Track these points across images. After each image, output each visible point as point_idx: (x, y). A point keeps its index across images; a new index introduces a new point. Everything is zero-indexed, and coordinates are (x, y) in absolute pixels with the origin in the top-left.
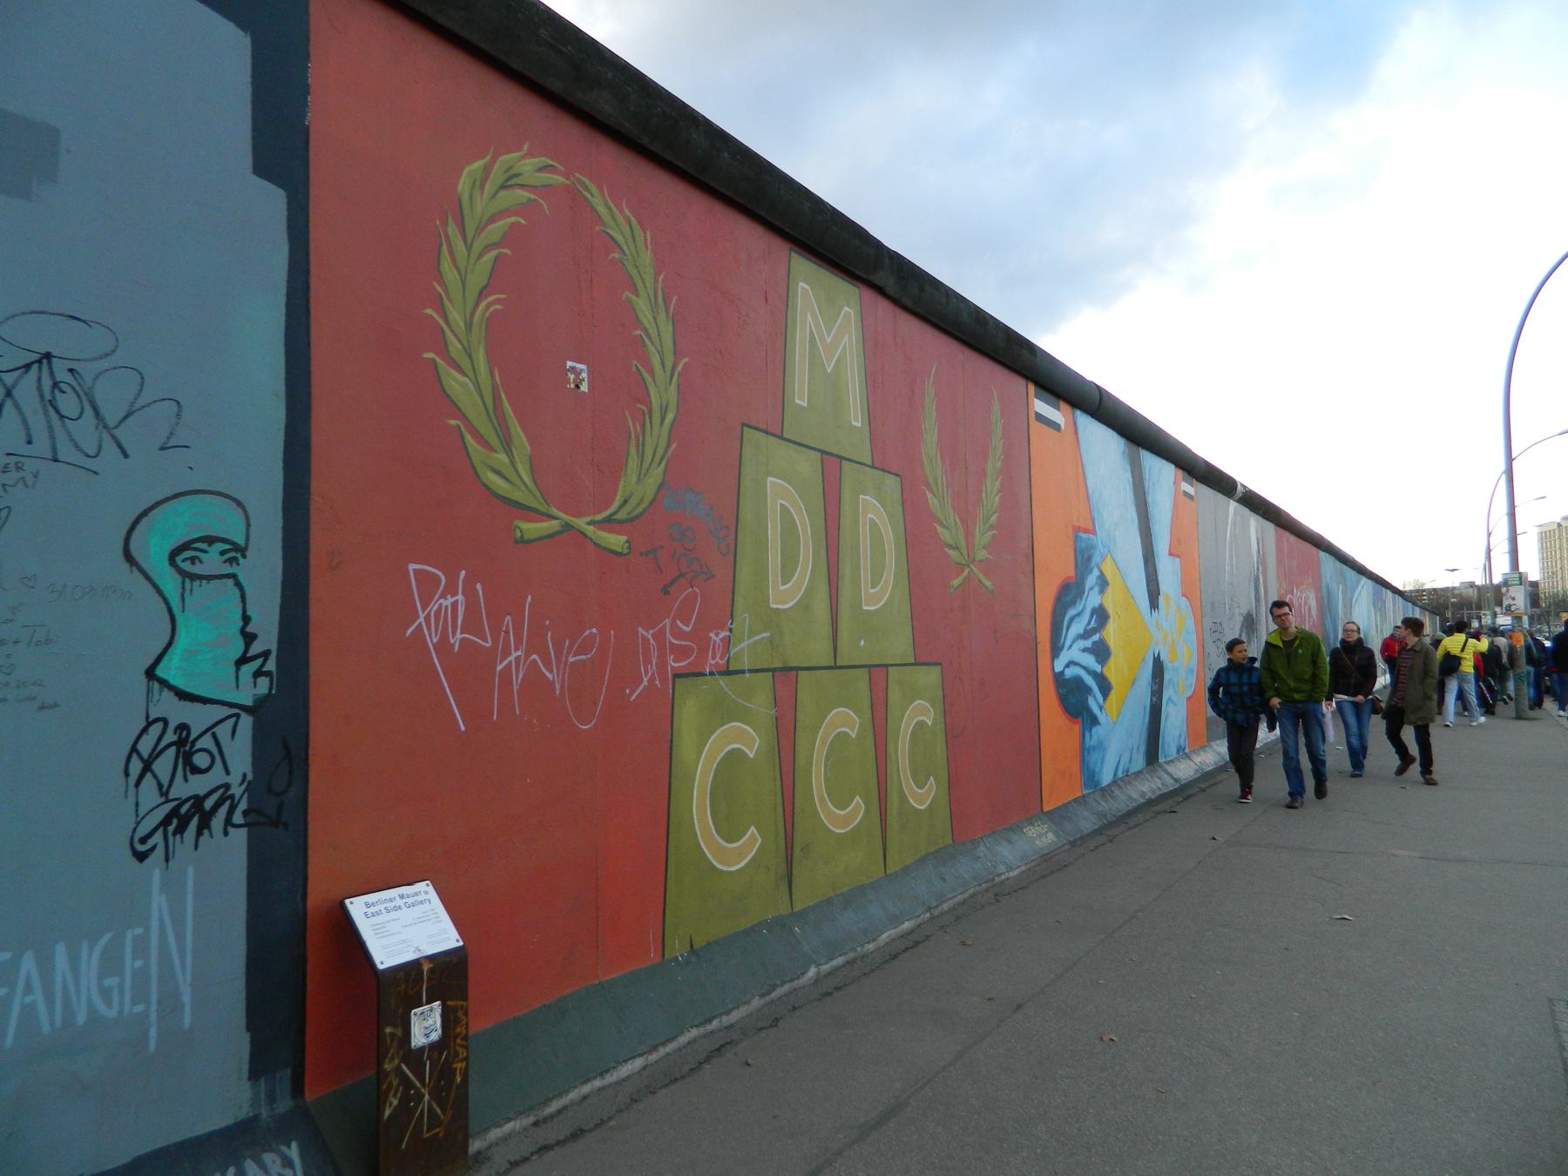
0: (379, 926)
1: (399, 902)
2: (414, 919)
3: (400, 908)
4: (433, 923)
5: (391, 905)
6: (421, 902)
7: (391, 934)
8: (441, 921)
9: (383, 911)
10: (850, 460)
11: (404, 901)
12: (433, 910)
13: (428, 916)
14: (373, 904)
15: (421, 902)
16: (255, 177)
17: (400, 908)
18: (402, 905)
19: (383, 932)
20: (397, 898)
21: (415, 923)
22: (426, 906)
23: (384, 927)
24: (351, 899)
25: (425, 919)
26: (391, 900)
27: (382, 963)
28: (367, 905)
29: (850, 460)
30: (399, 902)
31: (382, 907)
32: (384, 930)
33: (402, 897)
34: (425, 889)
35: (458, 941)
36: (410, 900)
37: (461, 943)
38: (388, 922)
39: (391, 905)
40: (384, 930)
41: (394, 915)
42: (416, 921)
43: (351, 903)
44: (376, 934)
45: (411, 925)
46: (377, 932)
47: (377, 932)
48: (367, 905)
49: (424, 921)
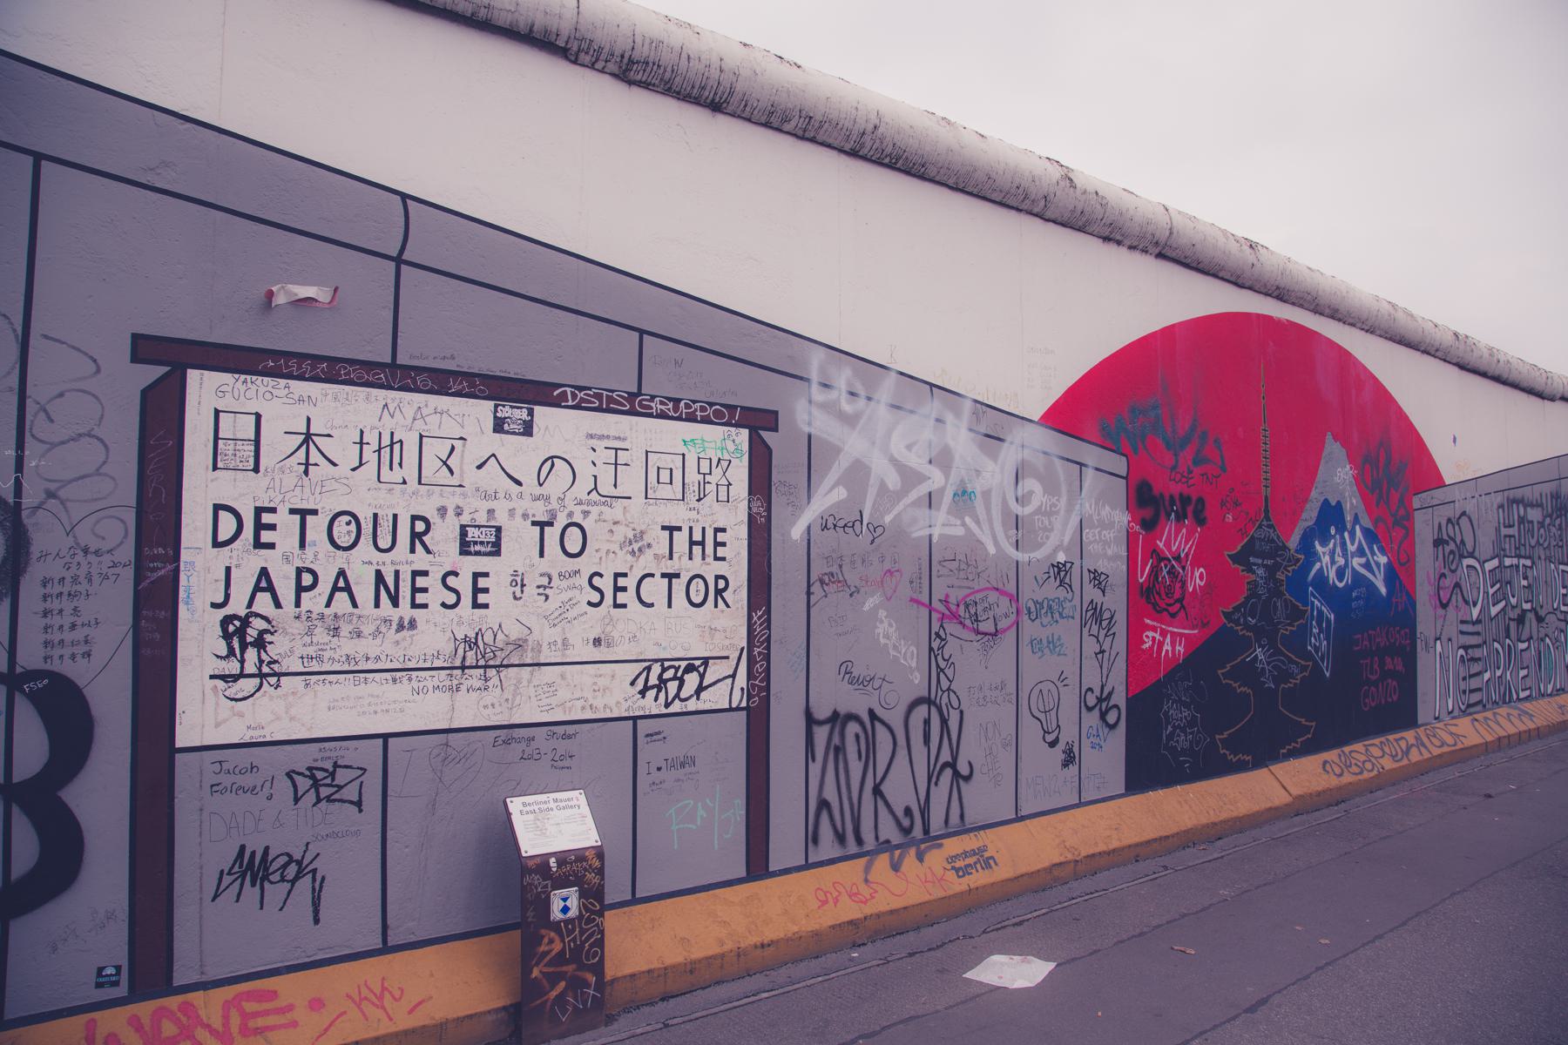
1: (552, 805)
3: (552, 809)
10: (728, 466)
17: (552, 809)
20: (551, 801)
22: (575, 810)
24: (512, 799)
26: (545, 802)
27: (526, 852)
29: (728, 466)
30: (552, 805)
31: (536, 808)
34: (578, 797)
35: (597, 842)
37: (599, 844)
43: (512, 802)
48: (524, 804)
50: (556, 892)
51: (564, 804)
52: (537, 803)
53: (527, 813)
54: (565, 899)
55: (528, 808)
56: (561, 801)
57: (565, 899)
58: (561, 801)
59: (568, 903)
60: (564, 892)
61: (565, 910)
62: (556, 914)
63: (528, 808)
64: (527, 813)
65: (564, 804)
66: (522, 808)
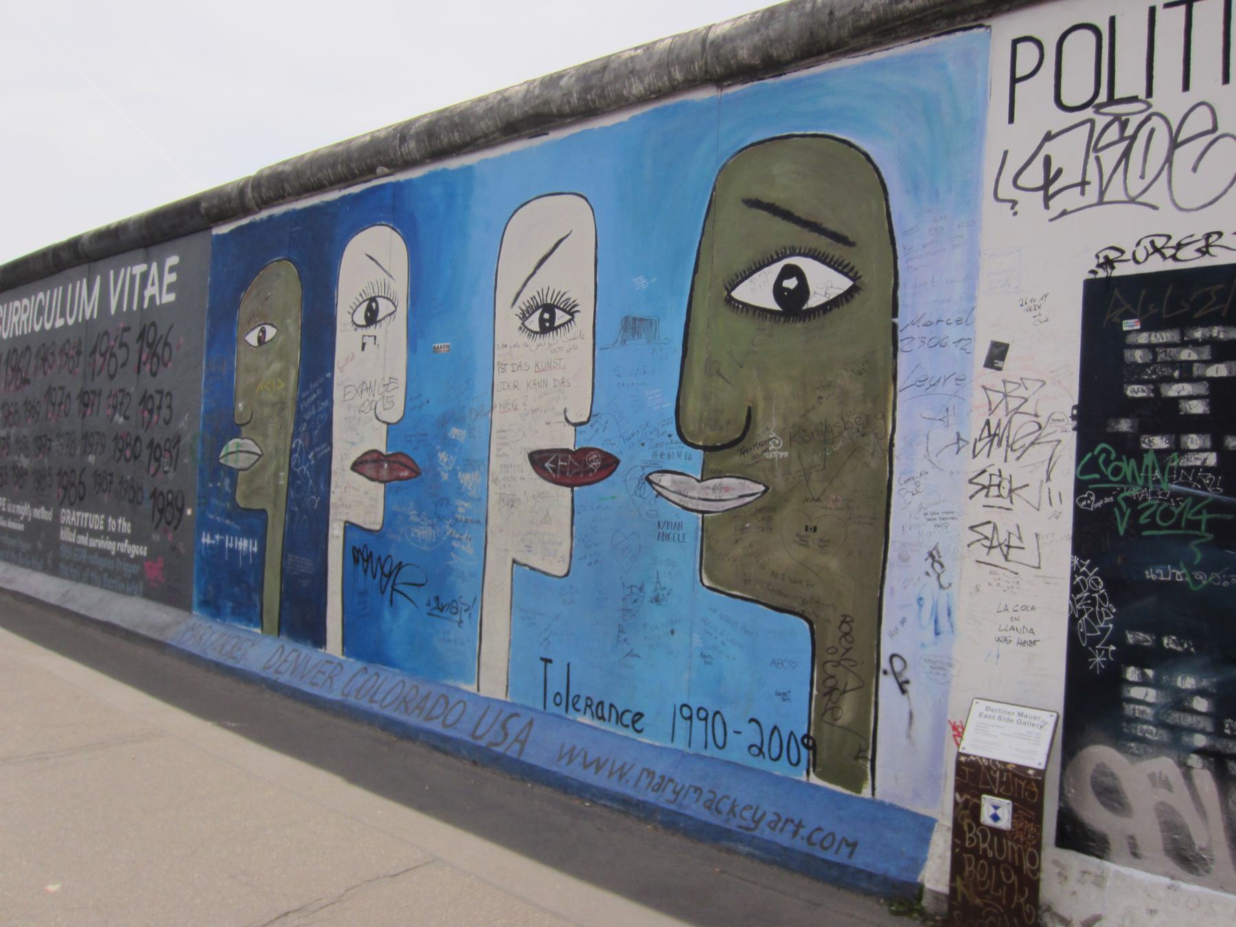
1: (1015, 718)
3: (1011, 721)
5: (1007, 716)
6: (1033, 725)
9: (996, 718)
15: (1033, 725)
16: (1015, 121)
17: (1011, 721)
18: (1015, 720)
20: (1016, 714)
22: (1035, 730)
26: (1009, 713)
28: (987, 708)
30: (1015, 718)
31: (997, 714)
33: (1020, 714)
36: (1024, 719)
38: (993, 726)
39: (1007, 716)
44: (977, 729)
51: (1026, 720)
52: (999, 710)
53: (986, 716)
54: (996, 808)
57: (996, 808)
59: (999, 812)
60: (997, 800)
61: (995, 818)
62: (986, 818)
64: (986, 716)
65: (1026, 720)
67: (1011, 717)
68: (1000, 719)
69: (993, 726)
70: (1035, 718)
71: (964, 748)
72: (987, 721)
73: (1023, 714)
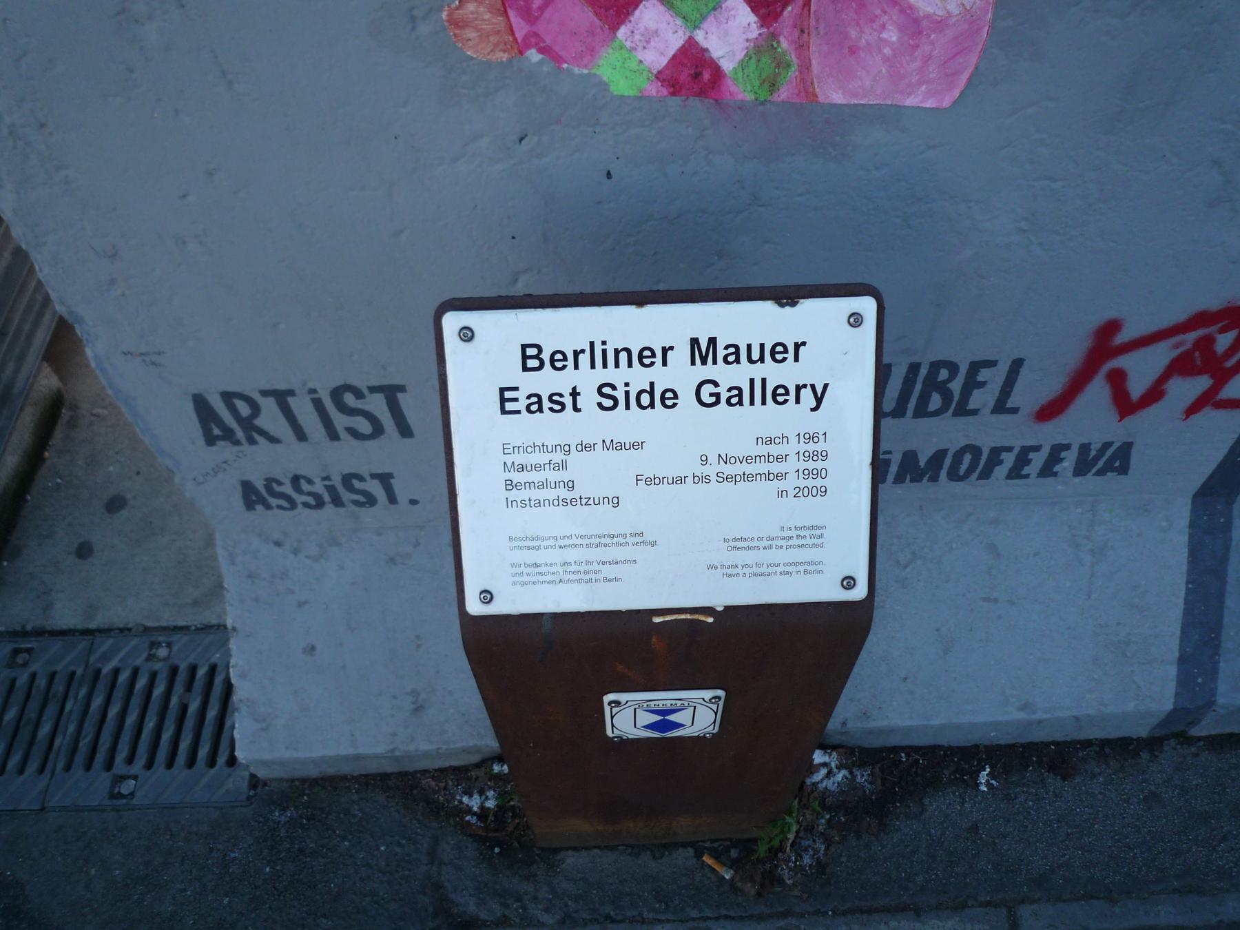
0: (542, 458)
2: (704, 460)
3: (669, 398)
4: (781, 494)
5: (638, 378)
6: (779, 395)
7: (573, 502)
8: (823, 491)
9: (589, 399)
11: (708, 371)
12: (812, 438)
13: (778, 459)
14: (557, 360)
15: (779, 395)
17: (669, 398)
19: (542, 485)
20: (681, 354)
21: (706, 479)
23: (562, 466)
25: (762, 467)
26: (645, 357)
31: (587, 379)
32: (553, 476)
38: (585, 447)
39: (638, 378)
40: (553, 476)
41: (626, 422)
42: (711, 470)
43: (467, 335)
44: (510, 485)
45: (681, 480)
46: (517, 477)
47: (517, 477)
48: (531, 357)
49: (746, 477)
50: (623, 697)
51: (739, 375)
52: (596, 355)
55: (547, 382)
56: (734, 355)
58: (734, 355)
63: (547, 382)
64: (536, 404)
65: (739, 375)
66: (512, 374)
67: (662, 377)
68: (608, 397)
69: (585, 447)
70: (778, 352)
71: (487, 596)
72: (547, 426)
73: (712, 341)
